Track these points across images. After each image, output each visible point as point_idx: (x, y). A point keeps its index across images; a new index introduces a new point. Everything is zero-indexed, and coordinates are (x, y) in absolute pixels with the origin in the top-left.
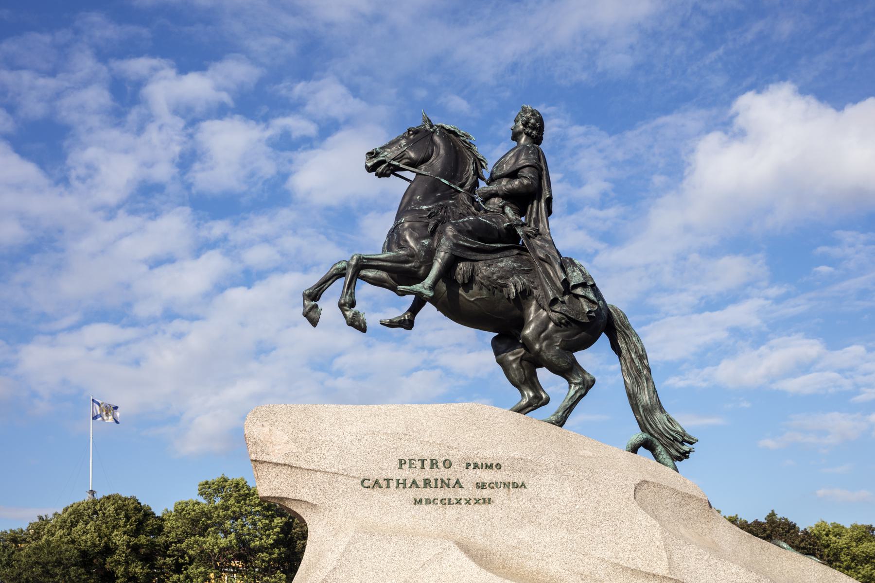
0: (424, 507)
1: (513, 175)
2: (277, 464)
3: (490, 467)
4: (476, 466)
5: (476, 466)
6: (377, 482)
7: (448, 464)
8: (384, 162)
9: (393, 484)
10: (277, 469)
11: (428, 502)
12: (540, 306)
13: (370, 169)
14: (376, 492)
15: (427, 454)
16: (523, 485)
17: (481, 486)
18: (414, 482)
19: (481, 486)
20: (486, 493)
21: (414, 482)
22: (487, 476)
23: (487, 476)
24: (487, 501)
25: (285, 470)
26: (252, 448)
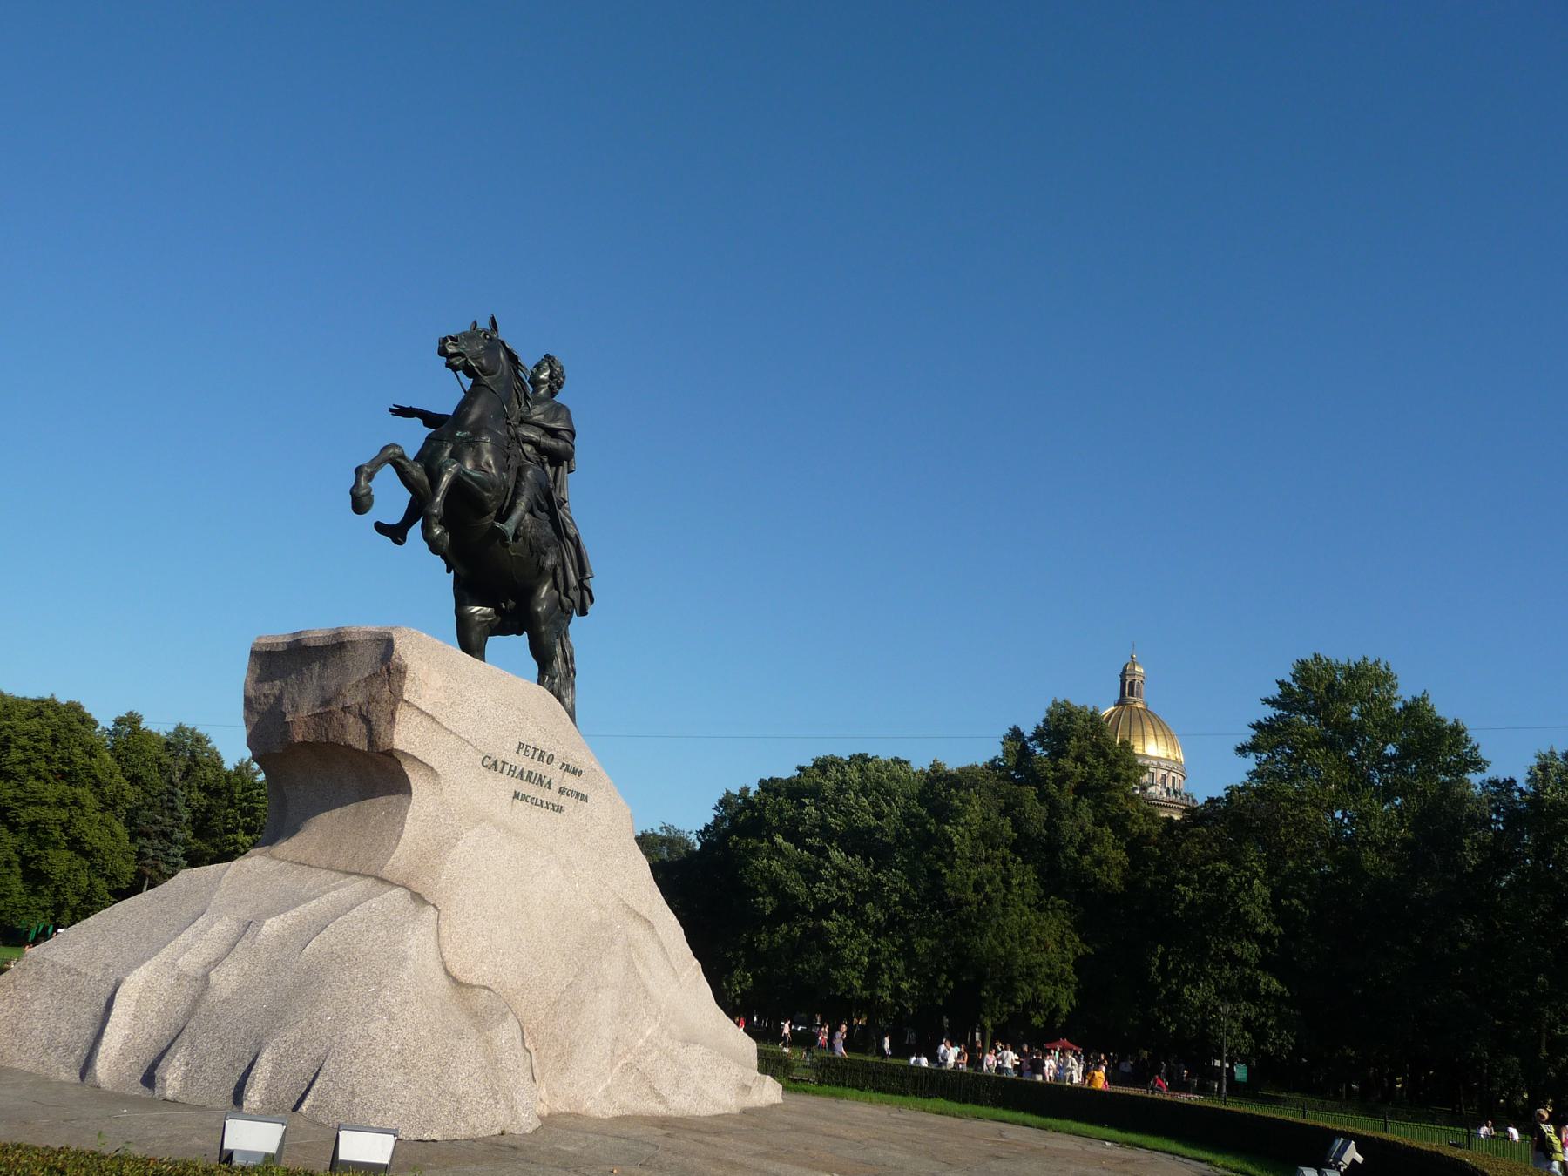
0: (518, 802)
1: (553, 433)
2: (423, 712)
3: (574, 772)
4: (567, 768)
5: (567, 768)
6: (495, 763)
7: (551, 759)
8: (461, 355)
9: (507, 768)
10: (420, 718)
11: (524, 798)
12: (555, 586)
13: (442, 352)
14: (491, 774)
15: (541, 745)
16: (584, 798)
17: (562, 791)
18: (521, 773)
19: (562, 791)
20: (563, 800)
21: (521, 773)
22: (570, 782)
23: (570, 782)
24: (560, 809)
25: (426, 723)
26: (408, 685)
